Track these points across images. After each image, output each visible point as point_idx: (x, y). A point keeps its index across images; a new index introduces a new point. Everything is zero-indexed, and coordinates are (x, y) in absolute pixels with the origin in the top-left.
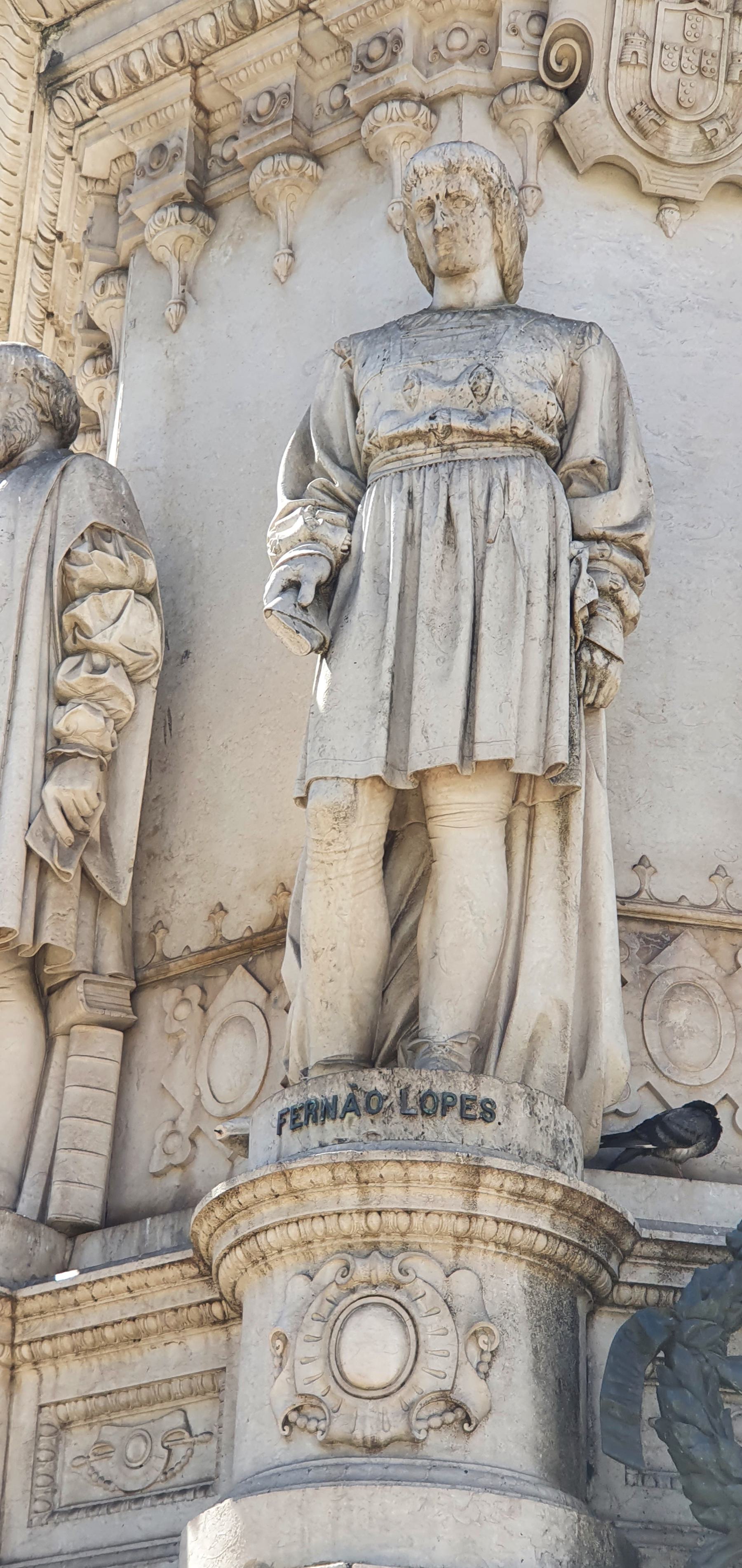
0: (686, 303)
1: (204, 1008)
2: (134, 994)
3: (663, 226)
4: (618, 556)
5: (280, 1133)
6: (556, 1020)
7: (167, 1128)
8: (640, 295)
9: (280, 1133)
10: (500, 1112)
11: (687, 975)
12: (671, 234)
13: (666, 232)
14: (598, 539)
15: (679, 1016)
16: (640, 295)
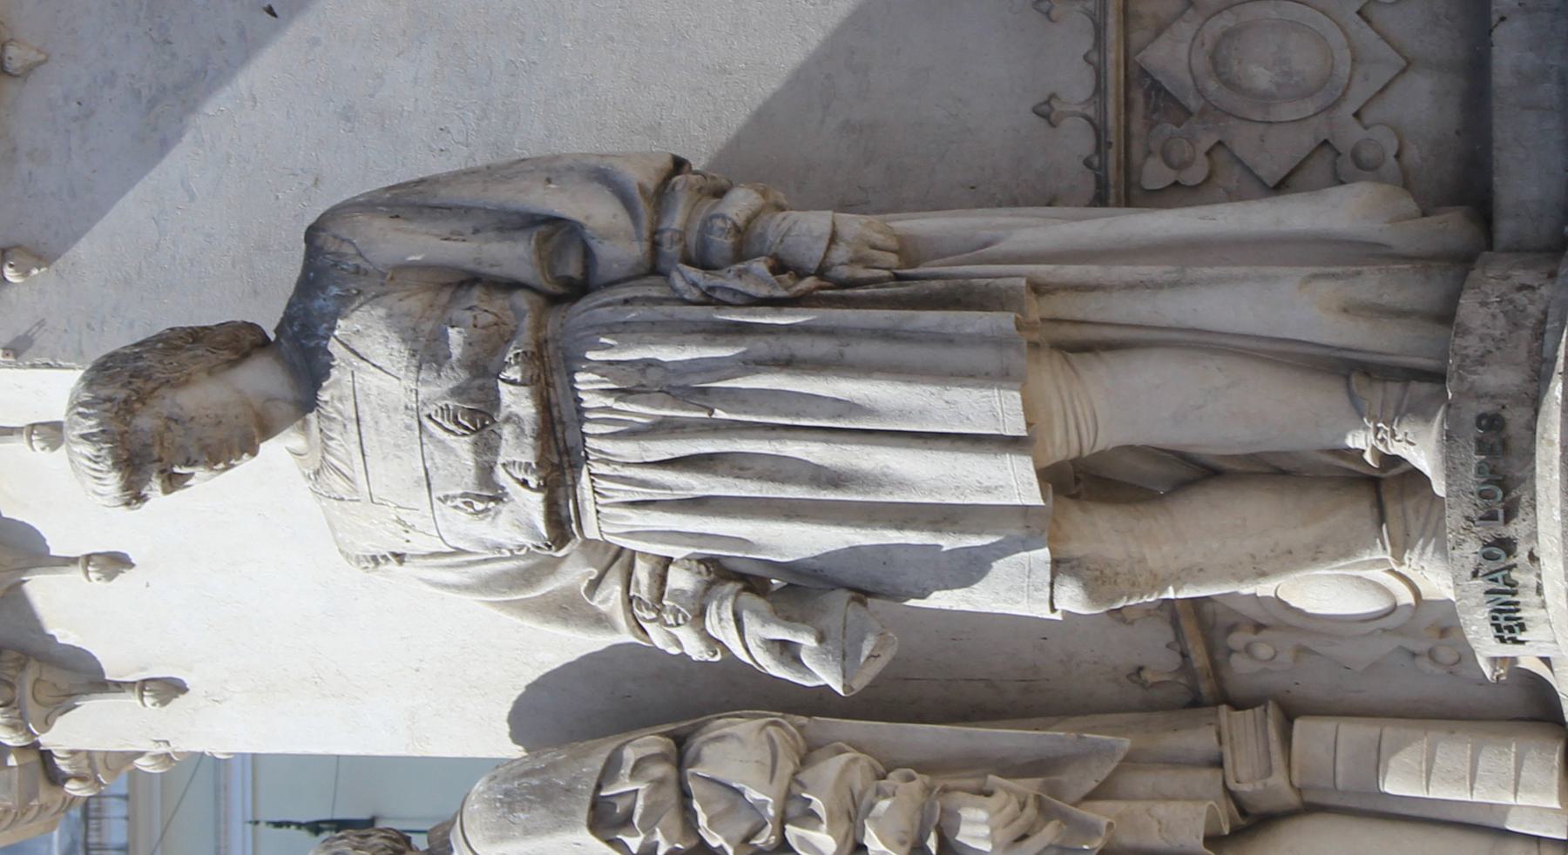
0: (155, 34)
1: (1259, 627)
2: (1238, 705)
3: (30, 69)
4: (676, 219)
5: (1522, 642)
6: (1325, 288)
7: (1424, 664)
8: (153, 102)
9: (1522, 642)
10: (1488, 407)
11: (1201, 63)
12: (42, 57)
13: (40, 63)
14: (655, 245)
15: (1261, 77)
16: (153, 102)
